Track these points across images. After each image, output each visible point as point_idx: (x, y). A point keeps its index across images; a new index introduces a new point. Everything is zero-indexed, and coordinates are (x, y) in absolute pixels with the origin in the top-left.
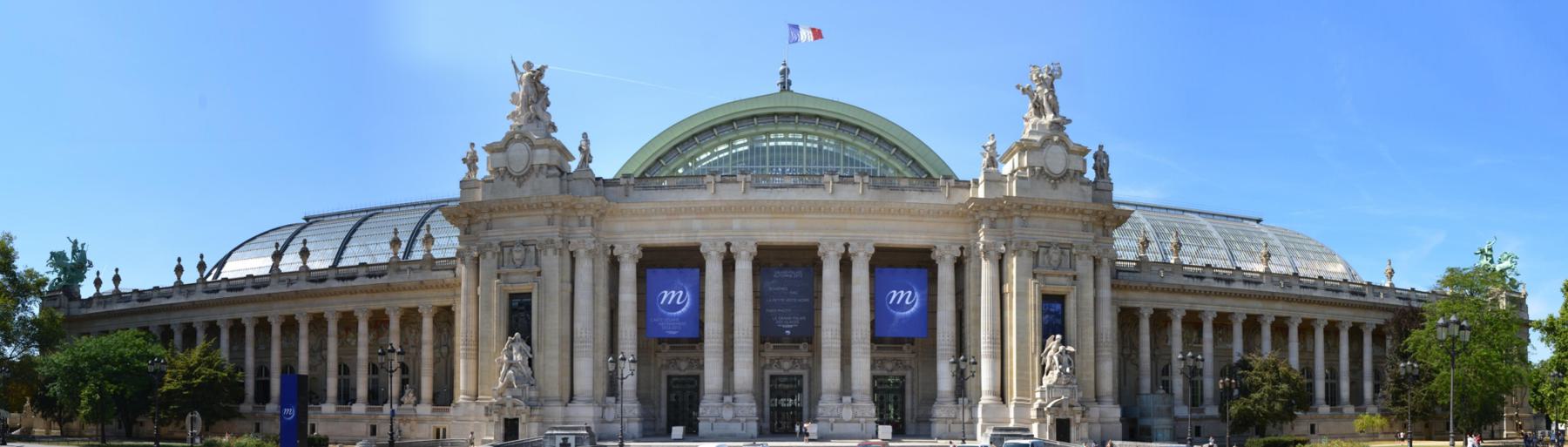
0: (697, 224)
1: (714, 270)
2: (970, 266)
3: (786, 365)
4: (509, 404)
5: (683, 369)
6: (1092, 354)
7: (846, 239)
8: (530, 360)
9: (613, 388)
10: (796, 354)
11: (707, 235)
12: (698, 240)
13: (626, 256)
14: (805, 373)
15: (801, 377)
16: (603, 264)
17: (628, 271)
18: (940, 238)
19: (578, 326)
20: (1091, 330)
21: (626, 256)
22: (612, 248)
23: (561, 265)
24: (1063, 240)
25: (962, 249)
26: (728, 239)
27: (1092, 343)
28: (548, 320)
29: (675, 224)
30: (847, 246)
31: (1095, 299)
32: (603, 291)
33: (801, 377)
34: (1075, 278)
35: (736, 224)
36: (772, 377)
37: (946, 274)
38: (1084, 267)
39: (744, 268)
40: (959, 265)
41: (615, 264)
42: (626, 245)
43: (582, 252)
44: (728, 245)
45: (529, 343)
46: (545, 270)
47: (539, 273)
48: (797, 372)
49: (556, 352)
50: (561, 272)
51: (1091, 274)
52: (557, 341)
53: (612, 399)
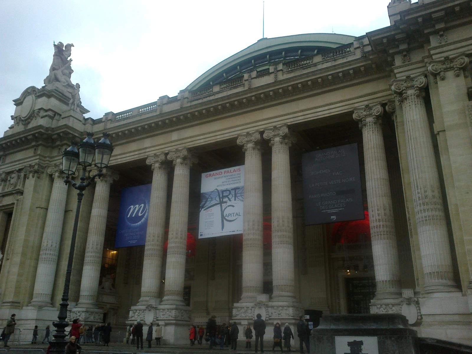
0: (147, 143)
7: (261, 128)
17: (102, 190)
25: (384, 105)
26: (166, 150)
29: (133, 146)
35: (175, 136)
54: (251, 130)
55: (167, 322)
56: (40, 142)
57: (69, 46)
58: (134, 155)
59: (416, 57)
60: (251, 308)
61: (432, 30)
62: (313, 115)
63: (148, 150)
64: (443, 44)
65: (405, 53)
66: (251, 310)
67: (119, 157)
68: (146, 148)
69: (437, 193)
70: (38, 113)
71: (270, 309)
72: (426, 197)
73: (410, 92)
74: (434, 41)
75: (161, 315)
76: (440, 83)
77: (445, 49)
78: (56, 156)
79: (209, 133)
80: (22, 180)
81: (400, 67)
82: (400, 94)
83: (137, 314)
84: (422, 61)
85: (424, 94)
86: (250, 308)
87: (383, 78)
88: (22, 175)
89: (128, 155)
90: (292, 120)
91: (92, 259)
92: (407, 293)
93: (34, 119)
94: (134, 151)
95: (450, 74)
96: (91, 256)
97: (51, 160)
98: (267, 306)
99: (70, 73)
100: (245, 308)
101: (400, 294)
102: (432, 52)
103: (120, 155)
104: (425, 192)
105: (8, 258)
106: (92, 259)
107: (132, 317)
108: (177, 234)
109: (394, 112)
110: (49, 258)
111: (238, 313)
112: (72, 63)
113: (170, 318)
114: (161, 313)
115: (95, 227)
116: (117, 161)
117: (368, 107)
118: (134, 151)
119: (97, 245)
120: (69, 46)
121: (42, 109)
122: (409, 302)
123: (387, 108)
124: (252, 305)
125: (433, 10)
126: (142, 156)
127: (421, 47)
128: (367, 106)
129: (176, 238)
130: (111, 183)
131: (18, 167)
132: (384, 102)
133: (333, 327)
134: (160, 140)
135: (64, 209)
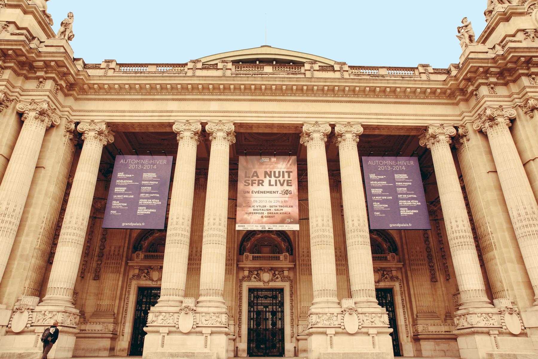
0: (172, 106)
1: (187, 152)
3: (266, 276)
10: (276, 264)
14: (286, 286)
15: (281, 290)
22: (77, 124)
25: (456, 128)
26: (204, 120)
30: (333, 126)
33: (281, 290)
35: (214, 106)
36: (251, 290)
40: (456, 144)
41: (77, 141)
44: (204, 125)
55: (214, 329)
58: (152, 116)
59: (501, 91)
60: (336, 315)
61: (526, 71)
66: (337, 316)
68: (172, 111)
70: (6, 27)
71: (360, 316)
75: (202, 321)
78: (33, 90)
79: (265, 112)
82: (492, 119)
83: (161, 317)
84: (510, 96)
86: (336, 314)
87: (453, 104)
91: (77, 238)
100: (329, 315)
106: (77, 238)
108: (220, 220)
110: (11, 229)
111: (319, 320)
113: (218, 325)
114: (203, 319)
115: (82, 197)
118: (153, 111)
119: (83, 220)
121: (14, 23)
124: (339, 310)
126: (164, 120)
127: (506, 84)
128: (442, 125)
129: (220, 224)
130: (104, 145)
132: (455, 125)
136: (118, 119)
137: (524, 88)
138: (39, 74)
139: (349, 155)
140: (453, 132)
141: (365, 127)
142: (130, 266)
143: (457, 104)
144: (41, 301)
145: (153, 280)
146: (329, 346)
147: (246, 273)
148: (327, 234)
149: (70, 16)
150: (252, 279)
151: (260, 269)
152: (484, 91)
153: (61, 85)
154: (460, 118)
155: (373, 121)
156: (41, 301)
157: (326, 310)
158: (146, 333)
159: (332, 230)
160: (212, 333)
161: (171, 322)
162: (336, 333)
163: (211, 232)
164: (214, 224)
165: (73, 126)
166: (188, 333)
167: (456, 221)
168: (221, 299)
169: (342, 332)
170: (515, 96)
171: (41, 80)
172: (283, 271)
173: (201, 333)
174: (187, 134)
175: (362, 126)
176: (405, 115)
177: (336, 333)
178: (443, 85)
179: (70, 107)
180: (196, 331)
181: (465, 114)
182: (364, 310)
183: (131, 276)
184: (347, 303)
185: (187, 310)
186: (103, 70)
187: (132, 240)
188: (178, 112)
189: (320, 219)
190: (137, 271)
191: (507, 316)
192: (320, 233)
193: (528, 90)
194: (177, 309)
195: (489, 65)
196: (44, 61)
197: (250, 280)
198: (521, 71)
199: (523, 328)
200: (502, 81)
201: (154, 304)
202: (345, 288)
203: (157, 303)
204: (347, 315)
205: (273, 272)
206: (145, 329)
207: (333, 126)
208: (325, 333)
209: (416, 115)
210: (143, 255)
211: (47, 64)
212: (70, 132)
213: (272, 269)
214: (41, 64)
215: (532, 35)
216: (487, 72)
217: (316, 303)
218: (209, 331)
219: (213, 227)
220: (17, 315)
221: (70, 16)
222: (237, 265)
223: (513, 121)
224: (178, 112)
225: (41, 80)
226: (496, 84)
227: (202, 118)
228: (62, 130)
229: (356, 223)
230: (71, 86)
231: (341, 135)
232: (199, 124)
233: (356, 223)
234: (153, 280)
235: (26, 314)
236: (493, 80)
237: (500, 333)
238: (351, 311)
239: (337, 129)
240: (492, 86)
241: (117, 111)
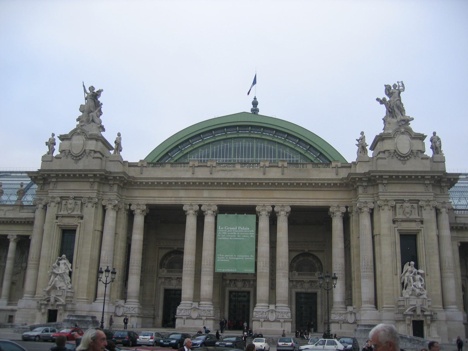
0: (182, 193)
1: (191, 222)
2: (353, 218)
4: (52, 300)
5: (173, 285)
6: (438, 274)
7: (273, 203)
8: (70, 274)
9: (124, 296)
11: (188, 200)
12: (182, 202)
13: (139, 211)
16: (123, 216)
17: (139, 221)
18: (334, 201)
19: (103, 253)
20: (436, 258)
21: (138, 211)
22: (130, 205)
23: (96, 214)
24: (412, 198)
25: (347, 207)
26: (200, 202)
27: (438, 268)
28: (84, 246)
29: (169, 193)
31: (438, 237)
32: (122, 232)
34: (422, 222)
35: (206, 194)
36: (231, 292)
37: (337, 224)
38: (428, 215)
39: (209, 220)
41: (131, 215)
42: (138, 205)
43: (110, 207)
45: (71, 261)
46: (86, 217)
47: (82, 218)
48: (247, 289)
49: (87, 269)
50: (95, 218)
51: (434, 219)
52: (88, 261)
53: (121, 302)
54: (267, 203)
56: (98, 180)
57: (100, 92)
59: (370, 190)
61: (381, 182)
62: (307, 203)
63: (183, 199)
64: (385, 191)
65: (365, 187)
67: (157, 199)
68: (182, 197)
69: (372, 264)
72: (368, 265)
73: (365, 209)
74: (381, 188)
75: (203, 314)
76: (381, 210)
77: (386, 194)
78: (108, 192)
79: (235, 198)
80: (80, 206)
81: (360, 194)
82: (361, 209)
83: (183, 311)
84: (373, 194)
85: (371, 212)
88: (79, 202)
89: (165, 199)
90: (293, 203)
92: (350, 309)
93: (85, 157)
94: (171, 197)
95: (386, 208)
96: (137, 269)
97: (103, 194)
98: (275, 311)
99: (101, 115)
101: (346, 308)
102: (380, 194)
103: (158, 197)
104: (368, 262)
105: (77, 267)
107: (179, 313)
108: (210, 262)
109: (352, 213)
111: (257, 314)
112: (102, 106)
113: (209, 315)
116: (155, 201)
117: (338, 207)
118: (171, 197)
120: (100, 92)
122: (351, 313)
123: (348, 209)
125: (384, 174)
126: (178, 202)
127: (373, 186)
131: (72, 195)
133: (364, 328)
134: (192, 193)
135: (114, 232)
136: (152, 202)
137: (378, 192)
138: (111, 182)
139: (283, 225)
140: (344, 210)
141: (292, 207)
142: (159, 277)
143: (351, 191)
144: (125, 302)
145: (173, 285)
146: (260, 326)
147: (228, 282)
148: (265, 271)
149: (119, 135)
150: (232, 285)
151: (236, 280)
152: (360, 190)
153: (121, 186)
154: (350, 200)
155: (298, 203)
156: (125, 302)
157: (261, 310)
158: (176, 318)
159: (268, 269)
160: (207, 319)
161: (187, 313)
162: (264, 321)
163: (205, 269)
164: (207, 265)
165: (128, 207)
166: (196, 319)
167: (336, 265)
168: (211, 303)
169: (267, 320)
170: (375, 195)
171: (111, 185)
172: (250, 281)
173: (201, 319)
174: (191, 212)
175: (291, 206)
176: (317, 199)
177: (264, 321)
178: (341, 181)
179: (127, 197)
180: (199, 318)
181: (353, 199)
182: (280, 310)
183: (159, 283)
184: (272, 307)
185: (195, 309)
186: (139, 168)
187: (159, 261)
188: (185, 197)
189: (262, 263)
190: (163, 280)
191: (349, 315)
192: (262, 271)
193: (380, 194)
194: (189, 308)
195: (362, 177)
196: (114, 177)
197: (230, 286)
198: (378, 182)
199: (355, 320)
200: (371, 184)
201: (179, 304)
202: (272, 299)
203: (180, 304)
204: (270, 313)
205: (244, 282)
206: (176, 316)
207: (273, 207)
208: (259, 321)
209: (324, 199)
210: (166, 270)
211: (115, 178)
212: (127, 210)
213: (243, 280)
214: (112, 178)
215: (392, 155)
216: (360, 179)
217: (258, 306)
218: (204, 318)
219: (207, 266)
220: (118, 309)
221: (119, 135)
222: (222, 277)
223: (372, 210)
224: (185, 197)
225: (111, 186)
226: (366, 186)
227: (199, 201)
228: (123, 210)
229: (281, 265)
230: (125, 184)
231: (278, 212)
232: (197, 206)
233: (281, 265)
234: (173, 285)
235: (122, 308)
236: (365, 184)
237: (344, 323)
238: (272, 311)
239: (275, 209)
240: (365, 187)
241: (151, 197)
